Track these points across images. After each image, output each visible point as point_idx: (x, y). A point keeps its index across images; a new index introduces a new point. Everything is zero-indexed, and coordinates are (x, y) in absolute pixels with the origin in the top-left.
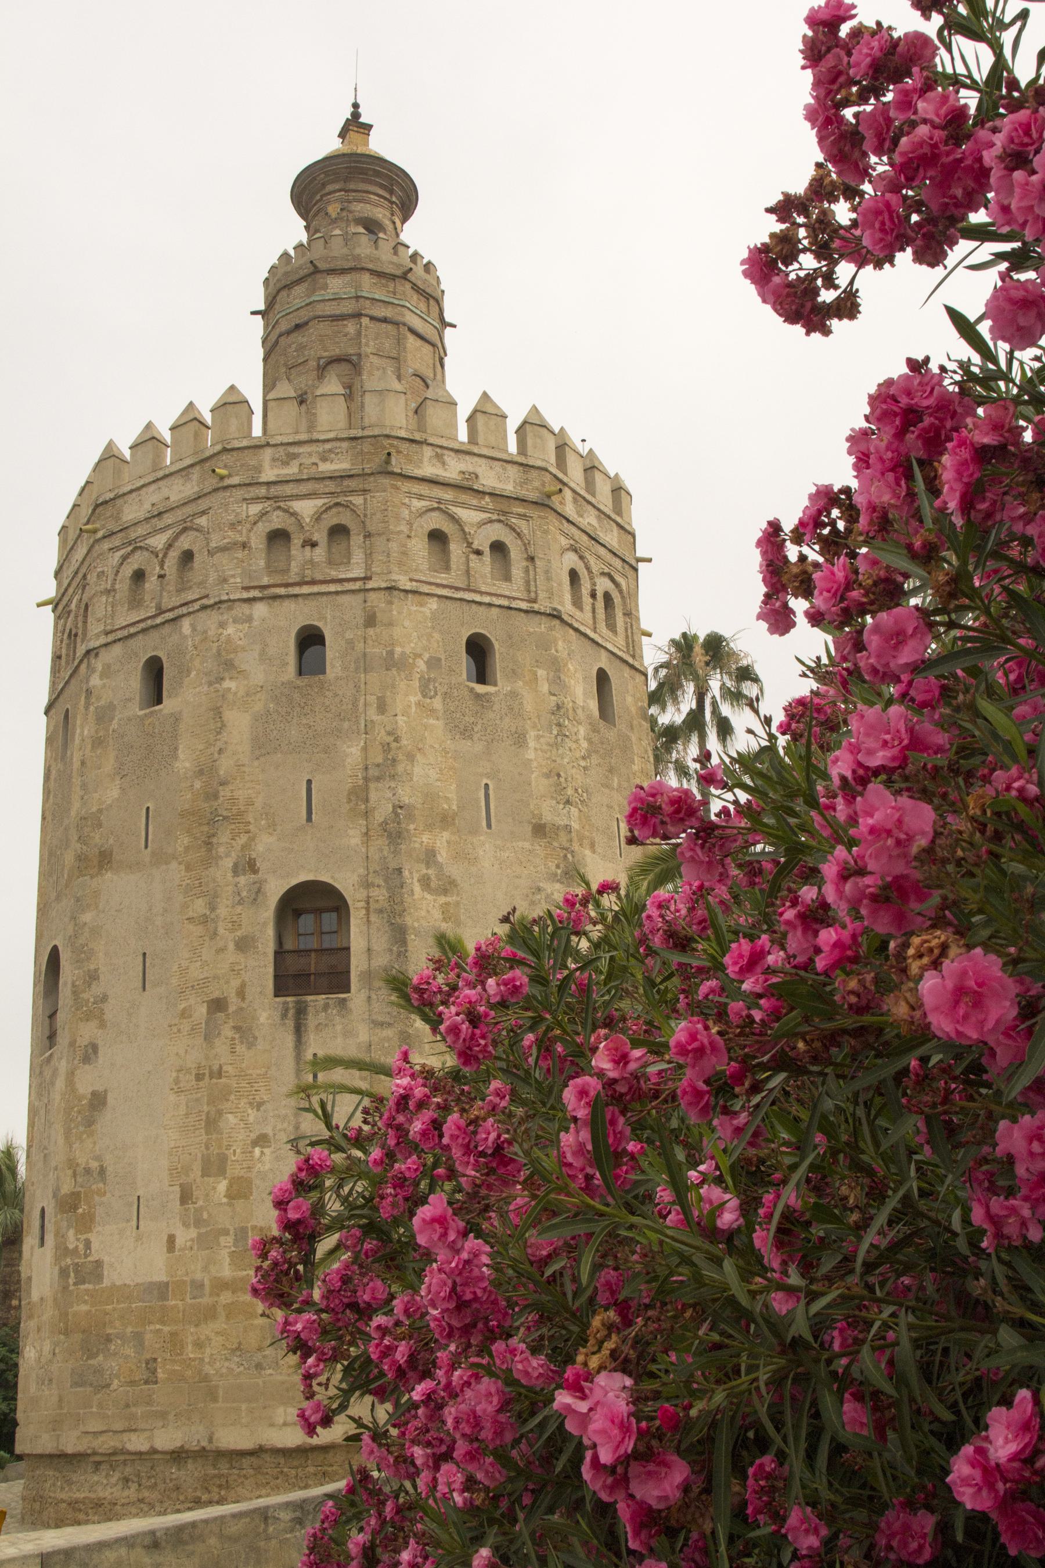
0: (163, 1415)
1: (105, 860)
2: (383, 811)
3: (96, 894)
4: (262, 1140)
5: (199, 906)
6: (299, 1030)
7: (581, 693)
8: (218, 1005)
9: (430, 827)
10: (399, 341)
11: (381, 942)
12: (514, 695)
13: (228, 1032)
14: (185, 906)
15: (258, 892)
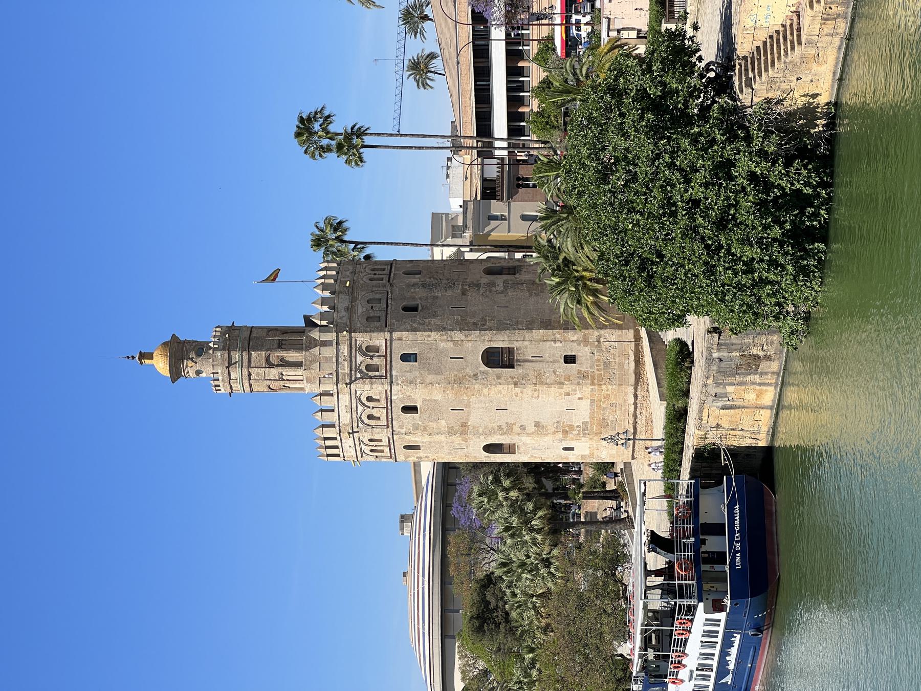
0: (625, 401)
1: (464, 425)
3: (474, 427)
4: (554, 372)
9: (466, 324)
10: (257, 338)
12: (420, 298)
13: (524, 382)
14: (485, 396)
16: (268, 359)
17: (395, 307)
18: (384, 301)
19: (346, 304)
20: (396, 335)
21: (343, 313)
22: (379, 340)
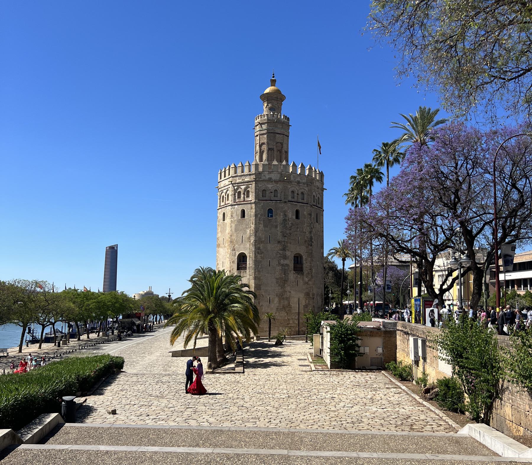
7: (291, 215)
9: (259, 244)
10: (275, 137)
12: (276, 218)
16: (263, 144)
17: (271, 205)
18: (276, 199)
19: (274, 178)
20: (253, 205)
21: (268, 177)
22: (252, 198)
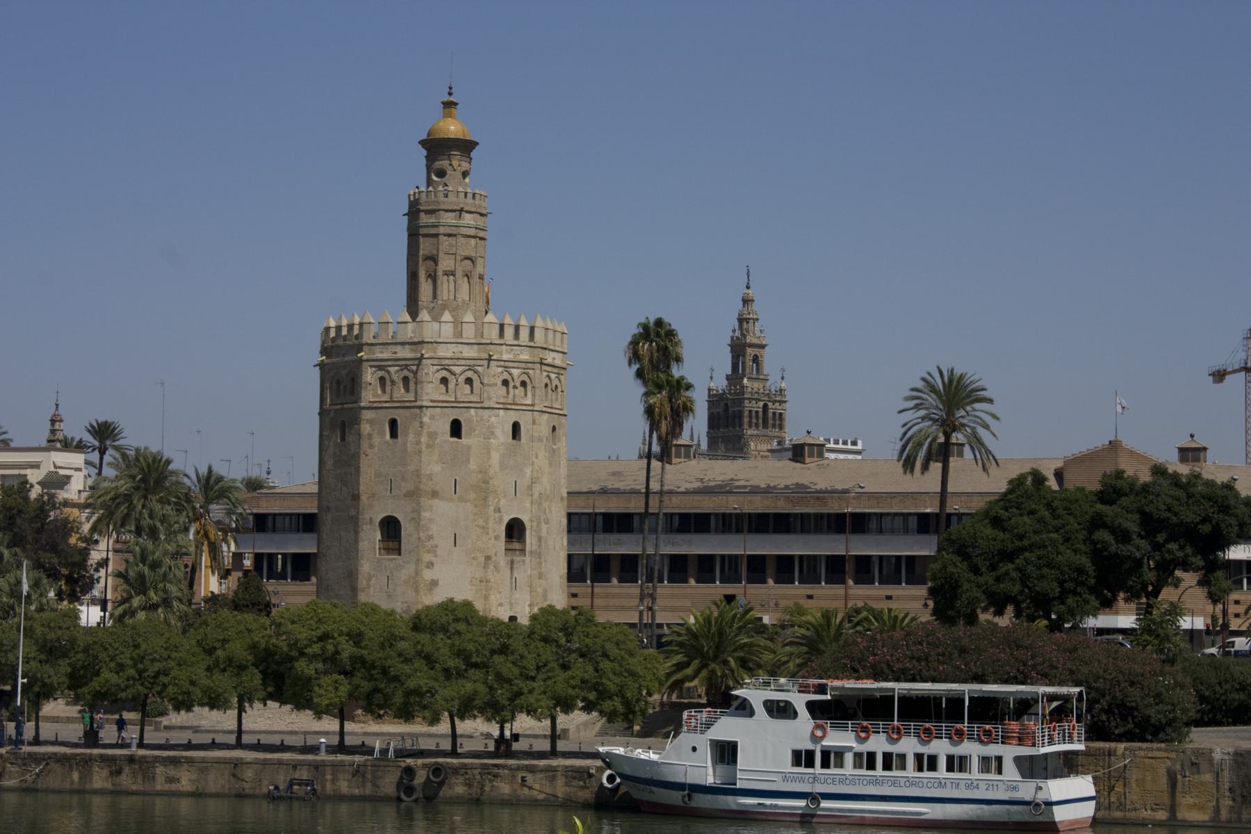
1: (435, 494)
2: (536, 495)
3: (431, 506)
4: (501, 605)
5: (481, 522)
6: (512, 569)
8: (488, 558)
11: (535, 541)
15: (501, 519)
